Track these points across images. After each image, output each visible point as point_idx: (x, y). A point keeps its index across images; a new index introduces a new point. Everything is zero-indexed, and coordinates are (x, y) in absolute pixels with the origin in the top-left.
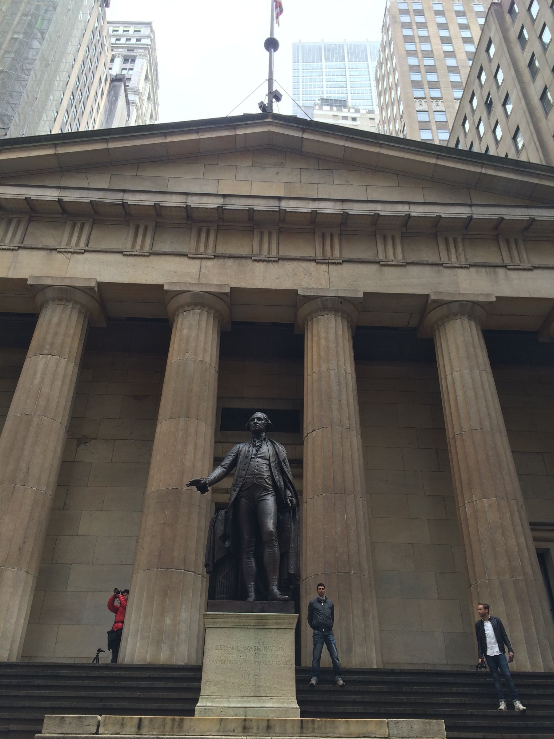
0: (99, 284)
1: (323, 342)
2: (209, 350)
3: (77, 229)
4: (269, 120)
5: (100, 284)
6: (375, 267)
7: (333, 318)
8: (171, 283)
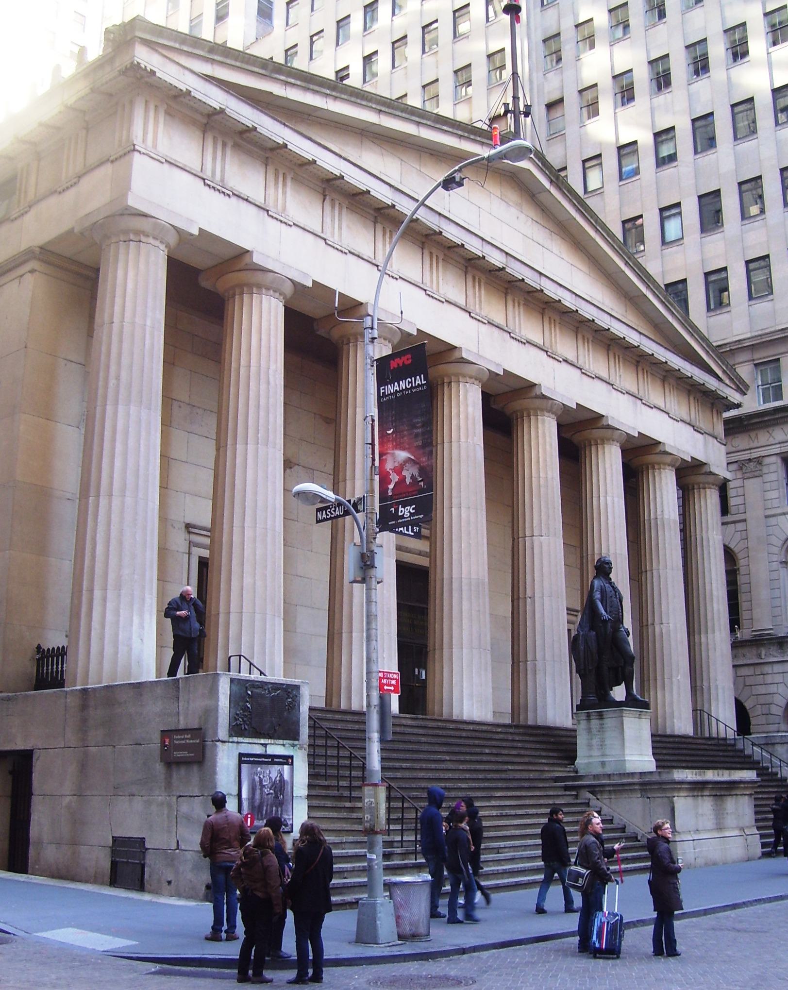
1: (548, 447)
6: (579, 371)
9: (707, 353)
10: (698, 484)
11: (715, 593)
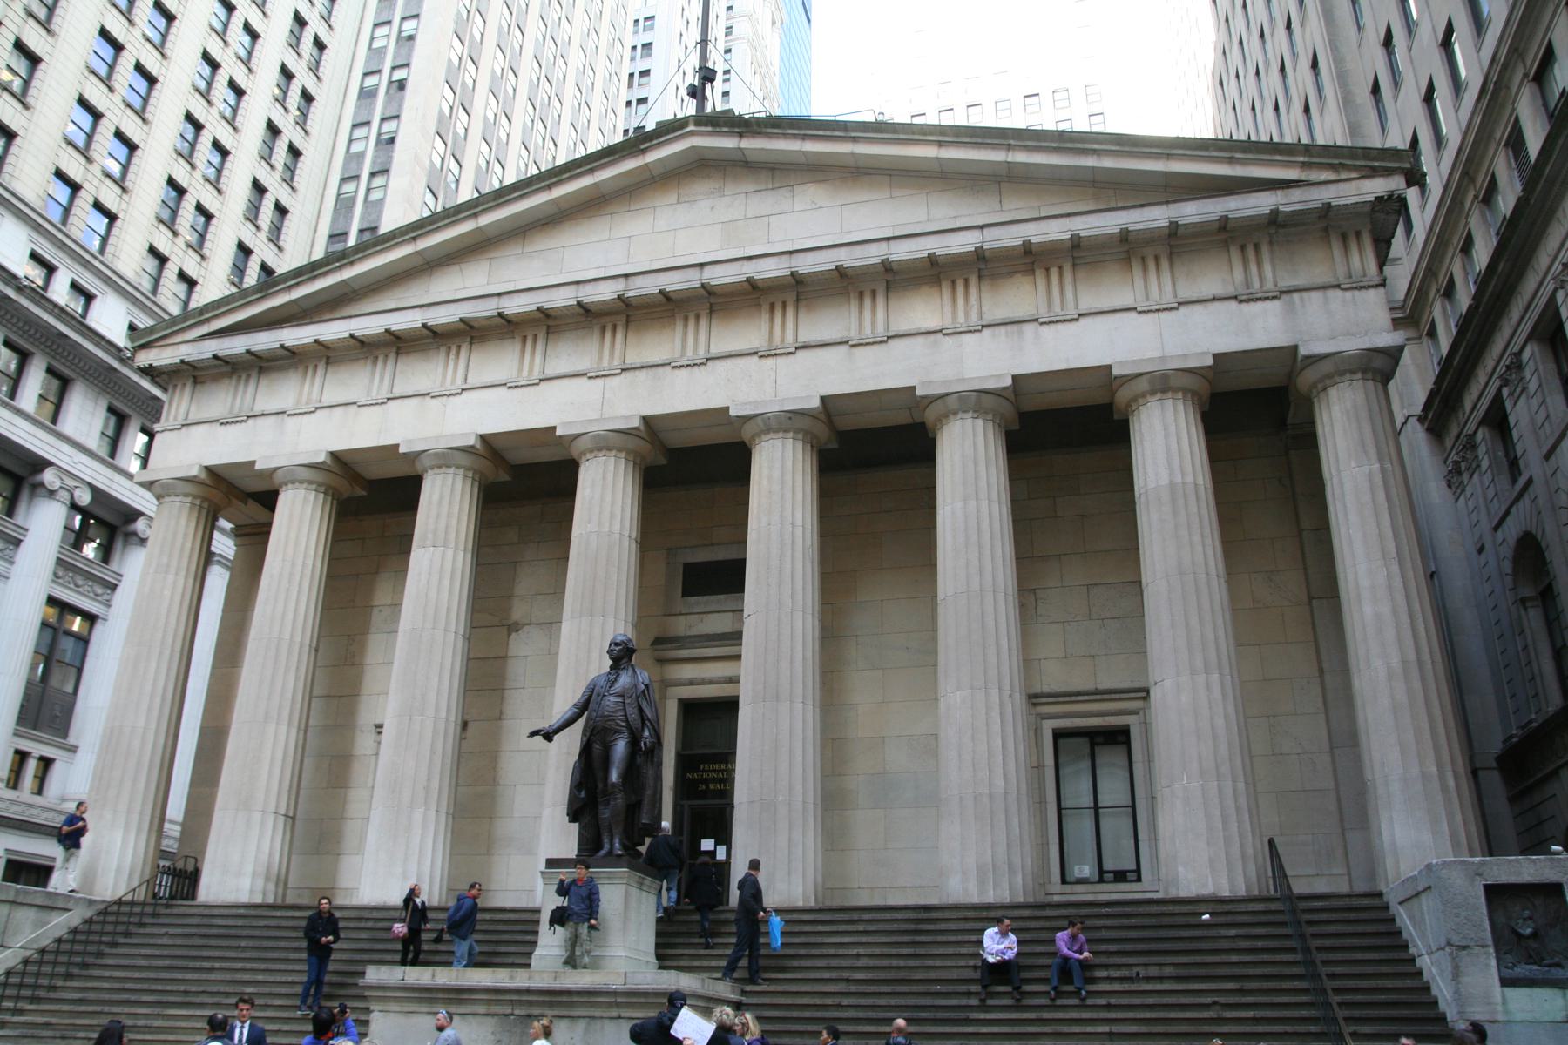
1: (765, 482)
2: (618, 512)
3: (452, 357)
4: (691, 128)
6: (843, 349)
7: (779, 443)
8: (565, 424)
9: (1231, 161)
10: (1314, 385)
11: (1365, 582)
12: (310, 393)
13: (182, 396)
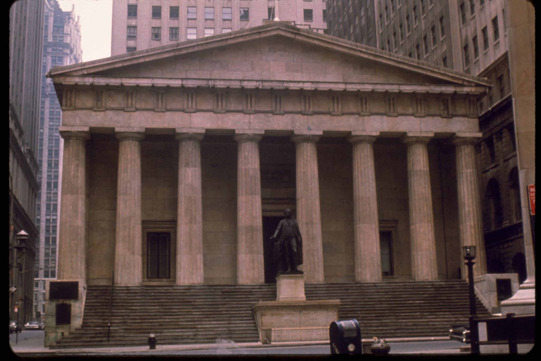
0: (207, 130)
5: (207, 130)
7: (309, 144)
11: (466, 202)
12: (132, 104)
13: (71, 95)
